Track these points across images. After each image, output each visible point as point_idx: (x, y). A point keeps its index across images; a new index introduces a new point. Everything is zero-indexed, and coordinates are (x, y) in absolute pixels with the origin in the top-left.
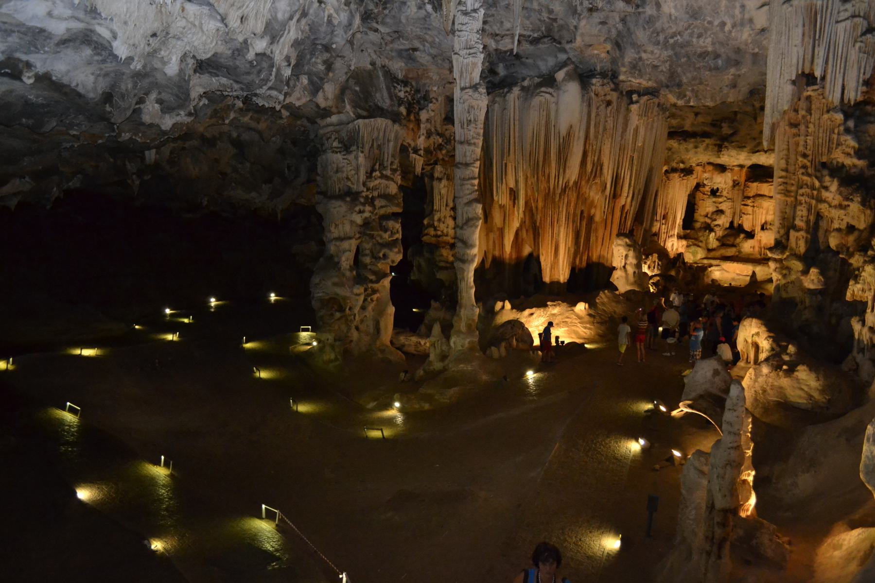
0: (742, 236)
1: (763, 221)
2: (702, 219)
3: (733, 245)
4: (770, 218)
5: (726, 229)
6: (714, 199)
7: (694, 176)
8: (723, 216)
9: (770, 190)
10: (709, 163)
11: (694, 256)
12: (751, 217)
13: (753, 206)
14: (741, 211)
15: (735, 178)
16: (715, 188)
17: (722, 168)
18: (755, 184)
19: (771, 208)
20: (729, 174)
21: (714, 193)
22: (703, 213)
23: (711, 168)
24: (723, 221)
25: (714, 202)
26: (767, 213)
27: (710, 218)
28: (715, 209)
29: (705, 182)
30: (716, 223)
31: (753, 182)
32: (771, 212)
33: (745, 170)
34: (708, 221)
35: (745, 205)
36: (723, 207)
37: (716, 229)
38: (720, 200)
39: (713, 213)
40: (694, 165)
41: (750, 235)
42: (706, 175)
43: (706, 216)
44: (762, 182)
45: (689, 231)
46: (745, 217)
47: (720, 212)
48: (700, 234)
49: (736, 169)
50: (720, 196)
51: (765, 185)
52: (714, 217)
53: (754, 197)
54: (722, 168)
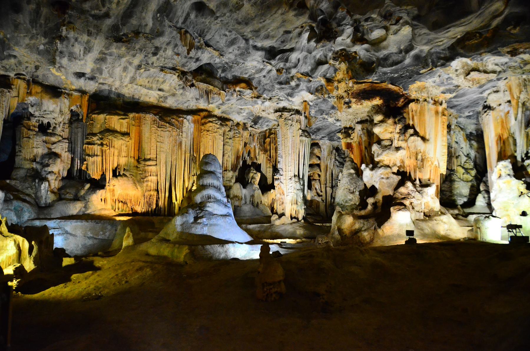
0: (88, 186)
1: (115, 165)
2: (27, 165)
3: (76, 199)
4: (123, 161)
5: (63, 179)
6: (44, 138)
7: (14, 93)
8: (59, 160)
9: (121, 125)
10: (35, 81)
11: (19, 216)
12: (100, 158)
13: (102, 145)
14: (84, 150)
15: (74, 108)
16: (45, 121)
17: (55, 91)
18: (102, 117)
19: (124, 148)
20: (67, 101)
21: (44, 129)
22: (29, 156)
23: (38, 89)
24: (59, 168)
25: (45, 142)
26: (119, 155)
27: (41, 164)
28: (46, 151)
29: (31, 110)
30: (49, 169)
31: (99, 114)
32: (124, 154)
33: (87, 98)
34: (34, 165)
35: (89, 143)
36: (58, 149)
37: (50, 177)
38: (54, 139)
39: (43, 156)
40: (12, 75)
41: (99, 184)
42: (31, 99)
43: (34, 160)
44: (110, 114)
45: (8, 181)
46: (91, 159)
47: (54, 155)
48: (27, 185)
49: (76, 94)
50: (53, 134)
51: (115, 118)
52: (46, 161)
53: (100, 133)
54: (55, 91)
